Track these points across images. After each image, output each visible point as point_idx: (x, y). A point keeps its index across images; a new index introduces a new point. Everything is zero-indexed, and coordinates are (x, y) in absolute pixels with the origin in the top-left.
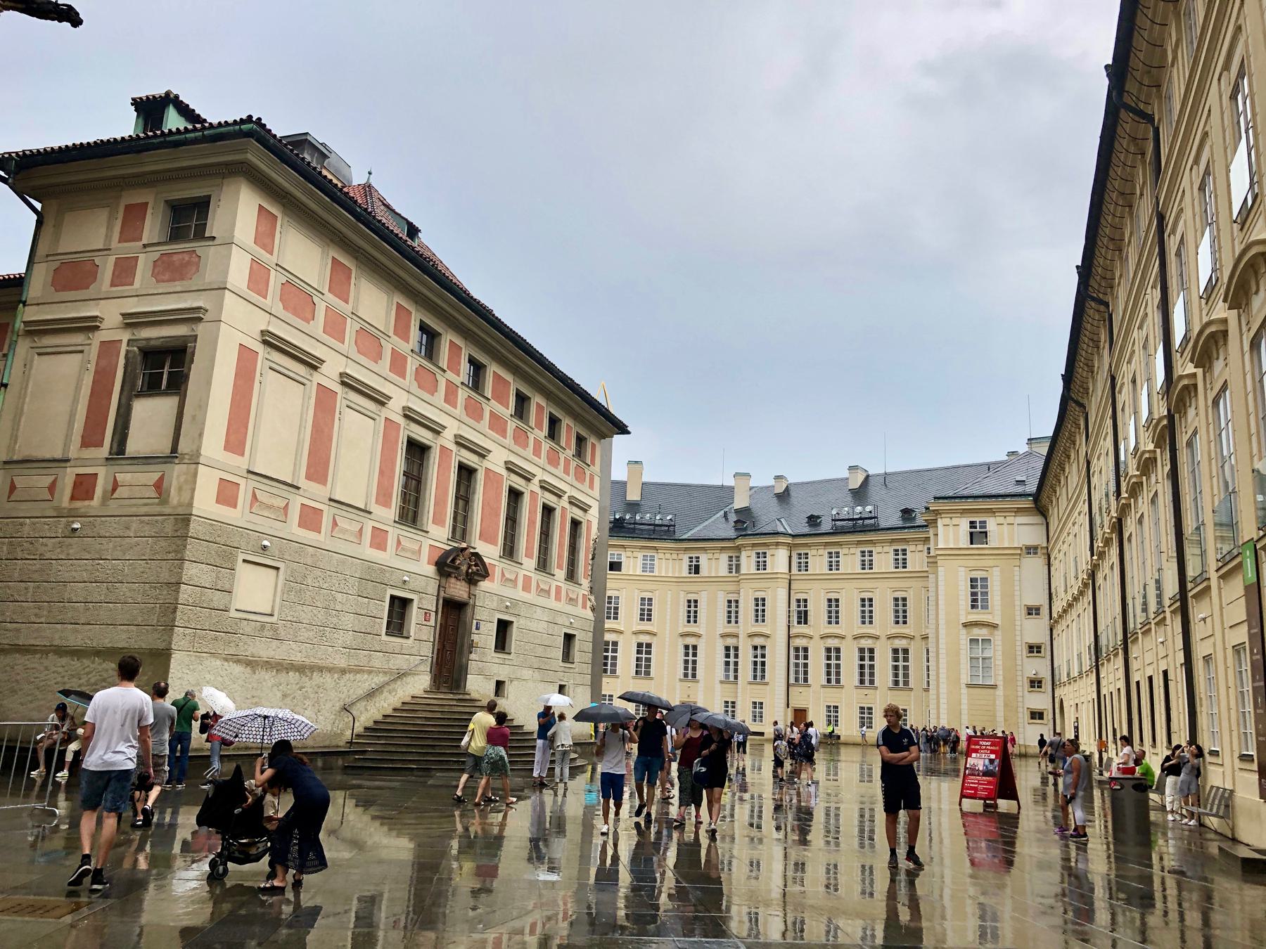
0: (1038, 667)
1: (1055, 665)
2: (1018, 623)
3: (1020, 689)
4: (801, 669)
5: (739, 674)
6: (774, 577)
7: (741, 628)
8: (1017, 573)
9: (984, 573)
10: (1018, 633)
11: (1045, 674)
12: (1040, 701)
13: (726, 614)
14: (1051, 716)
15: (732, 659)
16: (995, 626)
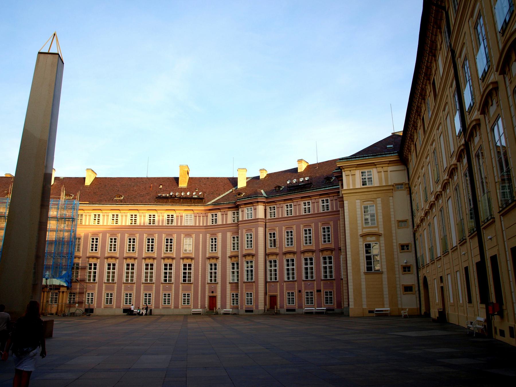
0: (407, 258)
1: (418, 255)
2: (394, 232)
3: (397, 273)
4: (273, 273)
5: (239, 278)
6: (256, 220)
7: (240, 252)
8: (391, 201)
9: (372, 202)
10: (394, 238)
11: (412, 262)
12: (409, 279)
13: (232, 245)
14: (417, 289)
15: (235, 270)
16: (380, 235)
